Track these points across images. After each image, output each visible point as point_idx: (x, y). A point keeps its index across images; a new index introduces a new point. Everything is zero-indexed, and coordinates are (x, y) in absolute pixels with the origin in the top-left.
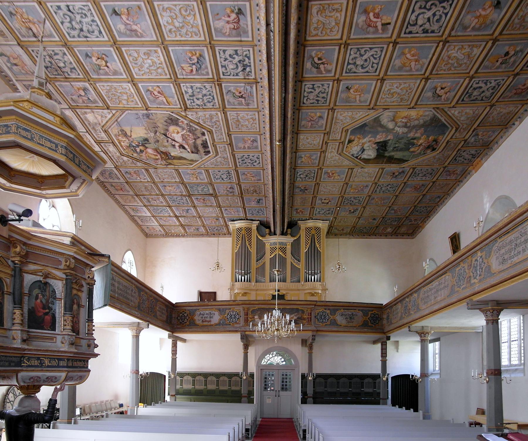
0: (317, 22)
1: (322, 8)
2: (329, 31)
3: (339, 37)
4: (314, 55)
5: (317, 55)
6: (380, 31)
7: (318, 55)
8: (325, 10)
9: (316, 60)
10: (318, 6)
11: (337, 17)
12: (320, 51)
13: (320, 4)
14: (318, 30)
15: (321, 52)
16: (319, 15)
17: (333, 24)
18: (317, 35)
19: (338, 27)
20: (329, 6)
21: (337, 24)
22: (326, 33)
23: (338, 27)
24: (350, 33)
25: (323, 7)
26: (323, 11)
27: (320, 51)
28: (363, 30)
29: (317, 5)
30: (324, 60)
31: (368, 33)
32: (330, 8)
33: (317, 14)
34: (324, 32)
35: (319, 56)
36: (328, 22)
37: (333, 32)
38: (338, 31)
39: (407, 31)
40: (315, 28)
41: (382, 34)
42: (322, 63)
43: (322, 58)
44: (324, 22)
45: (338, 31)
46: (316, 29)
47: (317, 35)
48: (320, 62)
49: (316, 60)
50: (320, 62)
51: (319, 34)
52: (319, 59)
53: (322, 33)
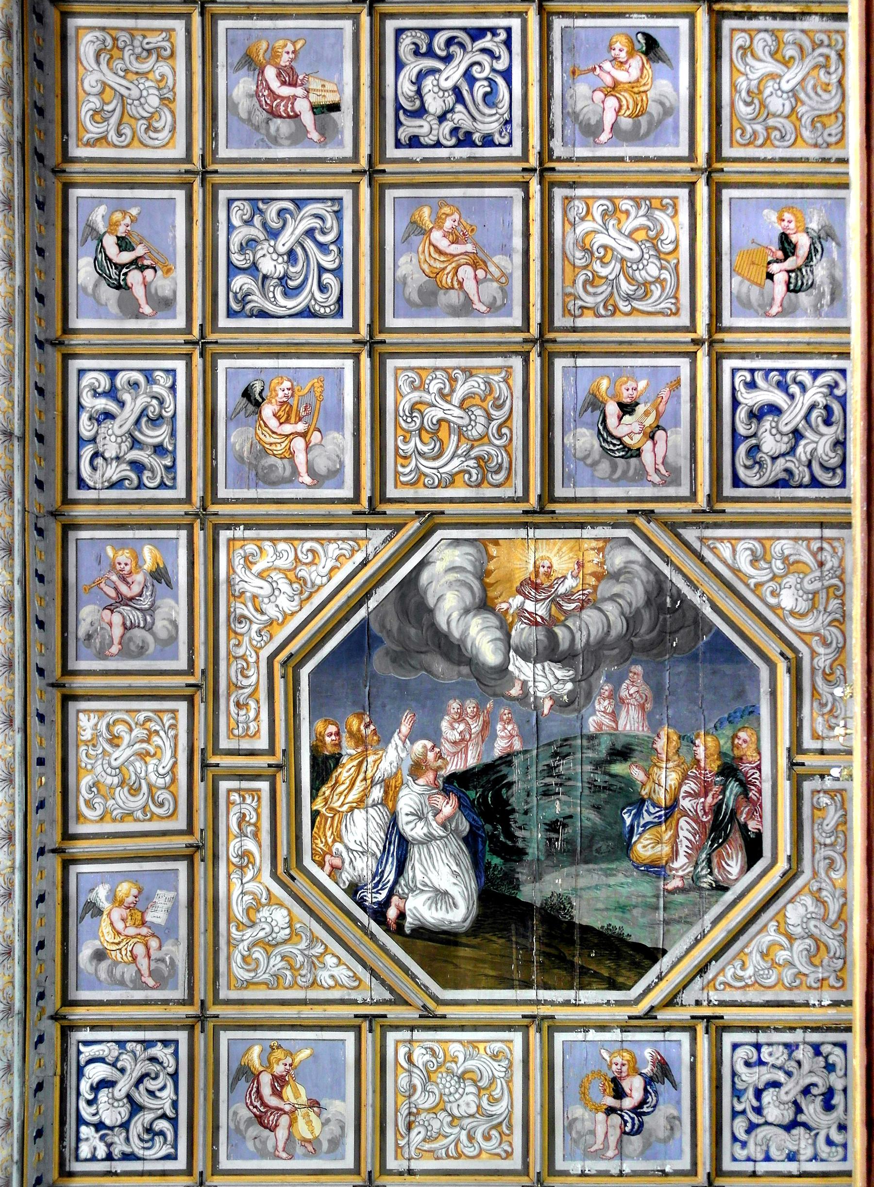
0: (98, 88)
1: (109, 41)
2: (141, 125)
3: (179, 152)
4: (101, 227)
5: (112, 226)
6: (314, 135)
7: (117, 224)
8: (122, 50)
9: (110, 242)
10: (98, 34)
11: (163, 76)
12: (120, 206)
13: (103, 29)
14: (106, 120)
15: (124, 213)
16: (104, 66)
17: (154, 101)
18: (102, 140)
19: (172, 113)
20: (133, 37)
21: (166, 101)
22: (134, 133)
23: (172, 113)
24: (215, 138)
25: (115, 39)
26: (115, 52)
27: (120, 206)
28: (257, 128)
29: (92, 28)
30: (140, 251)
31: (275, 141)
32: (137, 43)
33: (98, 62)
34: (127, 131)
35: (121, 231)
36: (135, 93)
37: (156, 130)
38: (173, 130)
39: (403, 135)
40: (96, 112)
41: (322, 144)
42: (137, 264)
43: (134, 240)
44: (125, 92)
45: (173, 130)
46: (98, 115)
47: (102, 140)
48: (126, 257)
49: (110, 242)
50: (126, 257)
51: (112, 136)
52: (124, 244)
53: (119, 134)
